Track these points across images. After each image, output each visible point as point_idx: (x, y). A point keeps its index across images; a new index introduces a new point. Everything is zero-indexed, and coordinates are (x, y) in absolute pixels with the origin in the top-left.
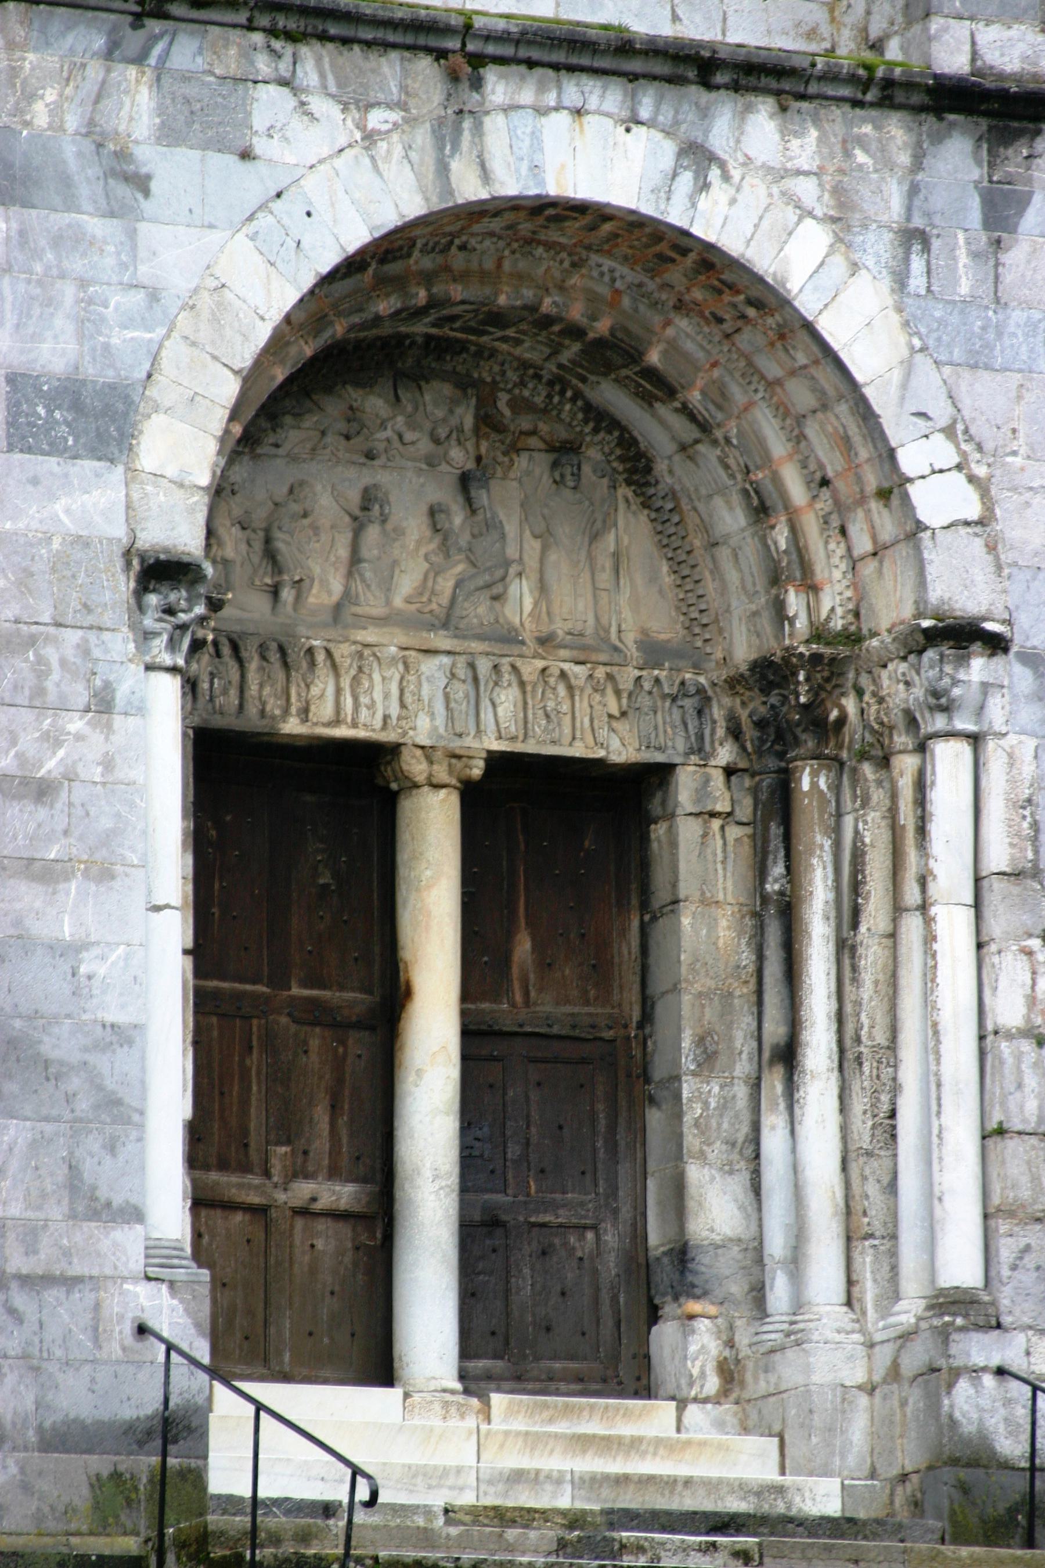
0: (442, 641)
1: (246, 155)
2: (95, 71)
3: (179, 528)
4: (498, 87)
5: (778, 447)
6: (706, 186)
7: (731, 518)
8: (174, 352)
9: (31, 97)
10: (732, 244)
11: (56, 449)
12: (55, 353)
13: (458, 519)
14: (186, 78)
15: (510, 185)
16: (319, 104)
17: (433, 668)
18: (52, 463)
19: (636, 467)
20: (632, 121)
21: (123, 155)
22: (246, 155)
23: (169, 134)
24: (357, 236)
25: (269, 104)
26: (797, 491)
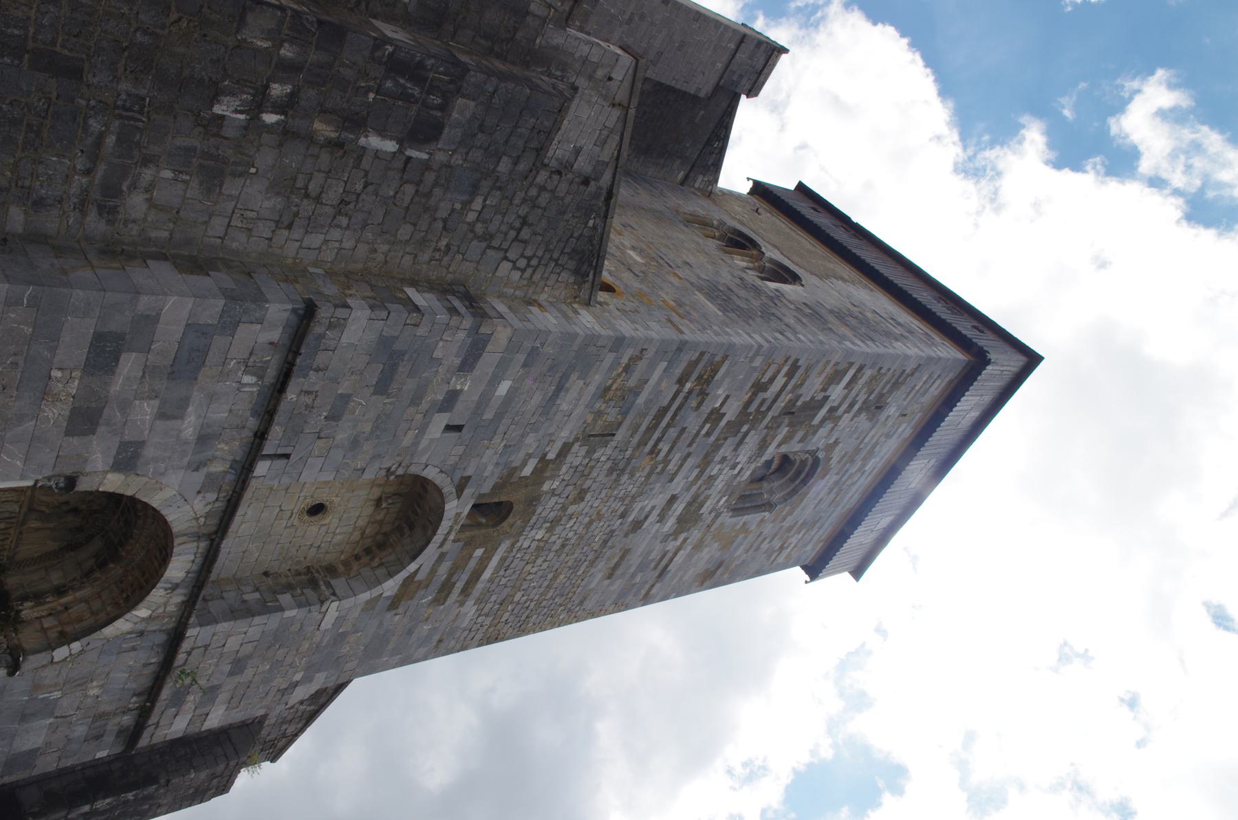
0: (24, 509)
1: (199, 492)
2: (231, 458)
3: (83, 485)
4: (204, 545)
5: (79, 594)
6: (166, 589)
7: (56, 578)
8: (145, 479)
9: (227, 444)
10: (148, 598)
11: (118, 453)
12: (149, 452)
13: (65, 508)
14: (223, 478)
15: (175, 550)
16: (209, 507)
17: (16, 508)
18: (114, 452)
19: (72, 547)
20: (188, 573)
21: (205, 465)
22: (199, 492)
23: (209, 475)
24: (169, 519)
25: (212, 496)
26: (64, 600)
